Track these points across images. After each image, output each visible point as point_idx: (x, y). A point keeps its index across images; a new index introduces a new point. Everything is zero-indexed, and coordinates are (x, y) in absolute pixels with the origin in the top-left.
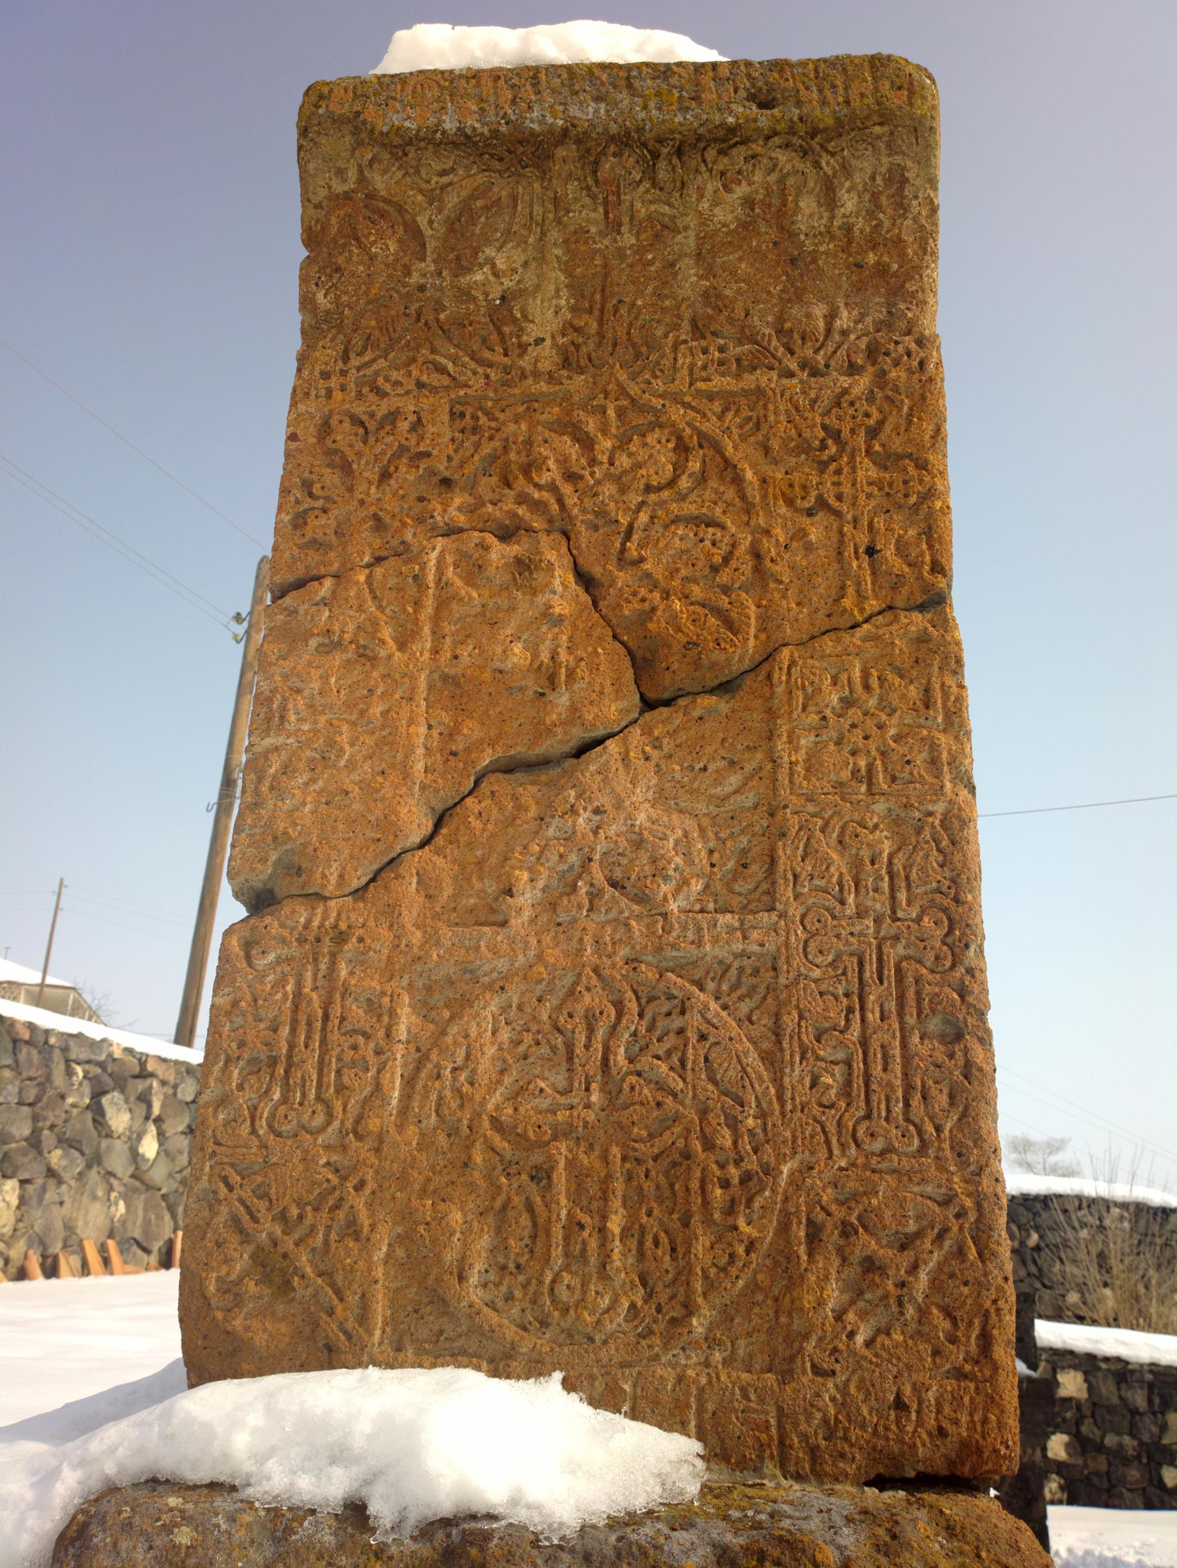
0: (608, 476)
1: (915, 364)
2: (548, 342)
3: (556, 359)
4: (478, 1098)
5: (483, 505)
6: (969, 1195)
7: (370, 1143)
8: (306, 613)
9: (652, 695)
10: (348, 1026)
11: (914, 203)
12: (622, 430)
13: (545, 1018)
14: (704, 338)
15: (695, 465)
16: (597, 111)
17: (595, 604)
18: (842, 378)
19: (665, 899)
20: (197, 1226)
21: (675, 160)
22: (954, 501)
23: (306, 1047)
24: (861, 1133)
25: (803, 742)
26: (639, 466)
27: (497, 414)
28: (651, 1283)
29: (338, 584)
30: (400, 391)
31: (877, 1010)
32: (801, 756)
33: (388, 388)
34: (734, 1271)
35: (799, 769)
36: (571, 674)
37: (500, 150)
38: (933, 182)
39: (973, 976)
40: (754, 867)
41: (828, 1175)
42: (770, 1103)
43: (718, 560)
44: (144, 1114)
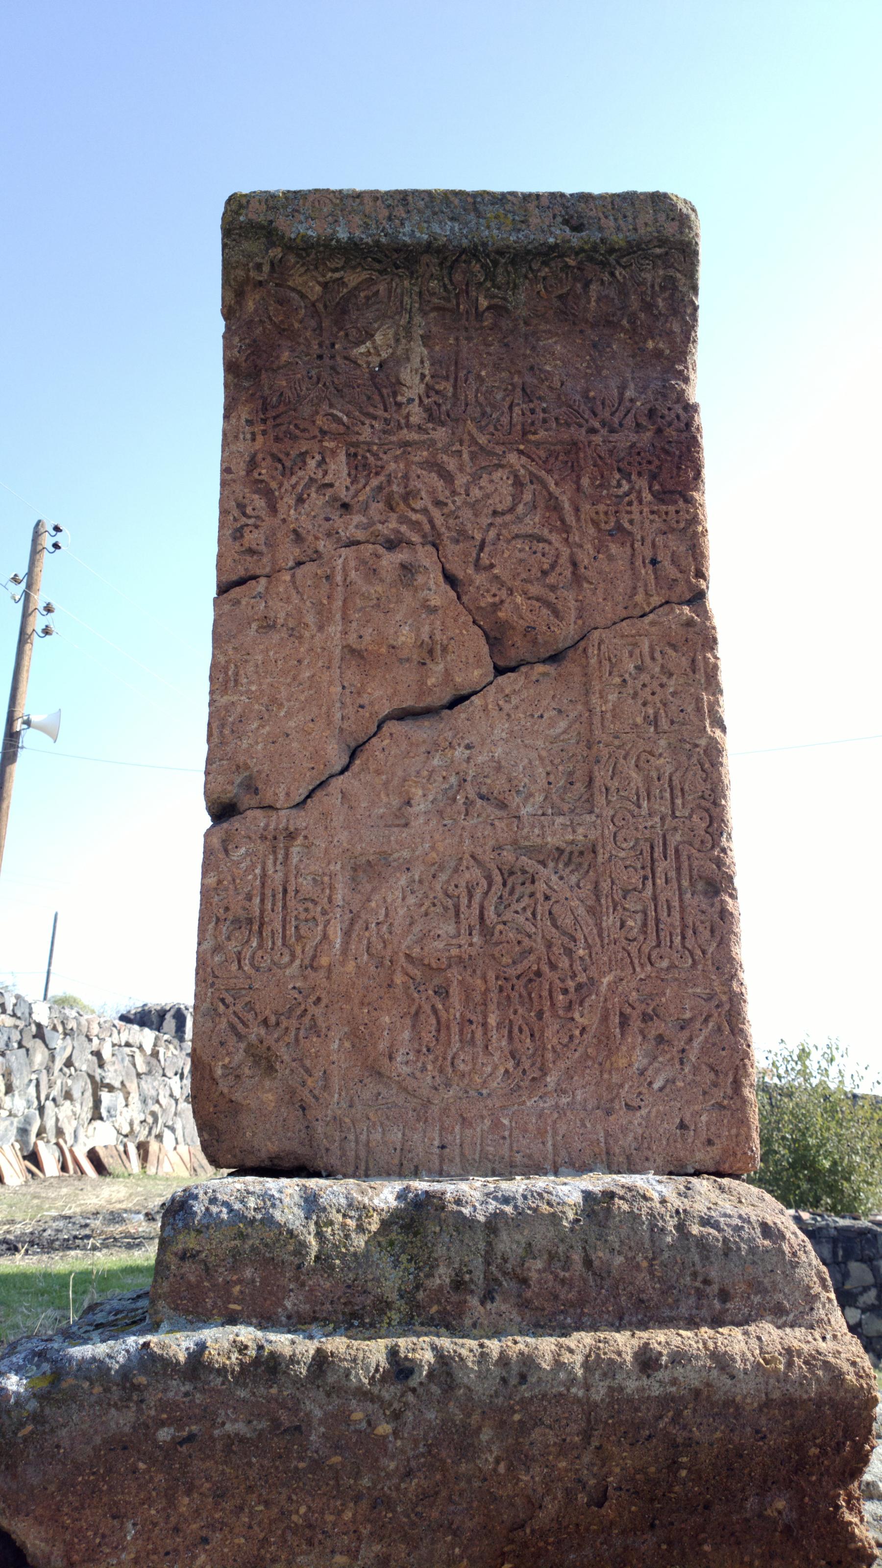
0: (465, 503)
2: (417, 401)
3: (425, 415)
4: (395, 941)
5: (374, 524)
6: (725, 993)
7: (322, 973)
8: (248, 603)
9: (501, 663)
10: (300, 896)
12: (474, 469)
13: (438, 887)
14: (531, 401)
15: (527, 497)
16: (452, 229)
17: (459, 598)
18: (631, 434)
19: (518, 806)
20: (204, 1033)
21: (510, 268)
22: (709, 525)
23: (273, 911)
24: (653, 957)
25: (610, 697)
26: (488, 496)
27: (381, 455)
28: (518, 1057)
29: (269, 583)
30: (307, 435)
34: (573, 1046)
35: (608, 715)
36: (444, 649)
37: (379, 256)
38: (695, 289)
39: (726, 853)
41: (633, 984)
42: (594, 939)
43: (546, 567)
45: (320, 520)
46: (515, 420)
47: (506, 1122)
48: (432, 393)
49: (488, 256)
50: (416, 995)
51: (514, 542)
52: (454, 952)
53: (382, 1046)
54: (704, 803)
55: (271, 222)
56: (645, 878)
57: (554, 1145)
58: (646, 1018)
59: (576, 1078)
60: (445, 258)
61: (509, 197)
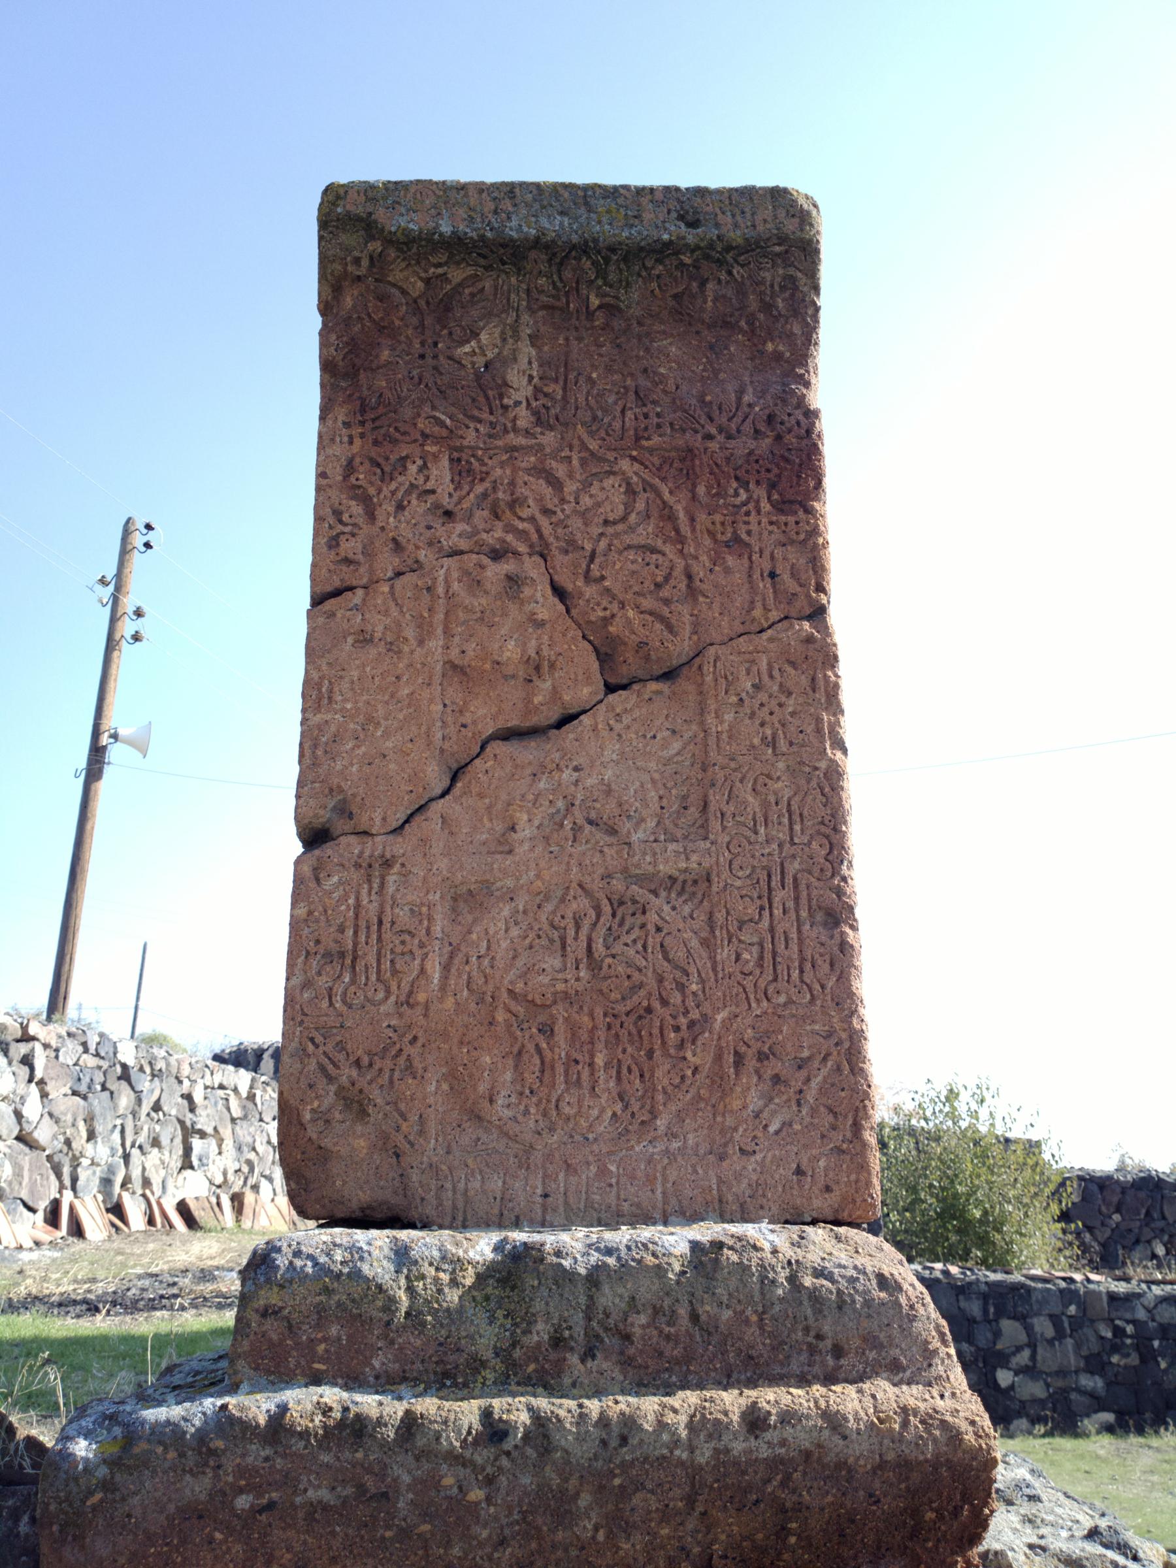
0: (575, 511)
2: (524, 404)
3: (533, 419)
4: (497, 976)
5: (478, 533)
6: (845, 1030)
7: (419, 1010)
8: (344, 616)
9: (612, 680)
10: (397, 928)
12: (584, 476)
13: (543, 918)
14: (645, 405)
15: (640, 505)
16: (561, 224)
17: (568, 611)
18: (749, 441)
19: (629, 832)
20: (292, 1074)
21: (622, 266)
22: (830, 537)
23: (367, 944)
25: (726, 717)
26: (598, 505)
27: (486, 460)
28: (626, 1099)
29: (367, 594)
30: (407, 438)
31: (781, 907)
32: (726, 726)
35: (724, 736)
36: (552, 666)
37: (484, 251)
38: (816, 289)
39: (846, 882)
40: (692, 809)
41: (749, 1021)
42: (707, 973)
43: (659, 579)
44: (27, 1077)
45: (421, 528)
46: (627, 424)
47: (613, 1168)
48: (540, 396)
49: (599, 252)
50: (519, 1033)
51: (626, 553)
52: (560, 987)
53: (482, 1088)
54: (823, 829)
55: (370, 214)
56: (762, 908)
57: (664, 1193)
58: (762, 1057)
59: (687, 1121)
60: (554, 254)
61: (622, 191)
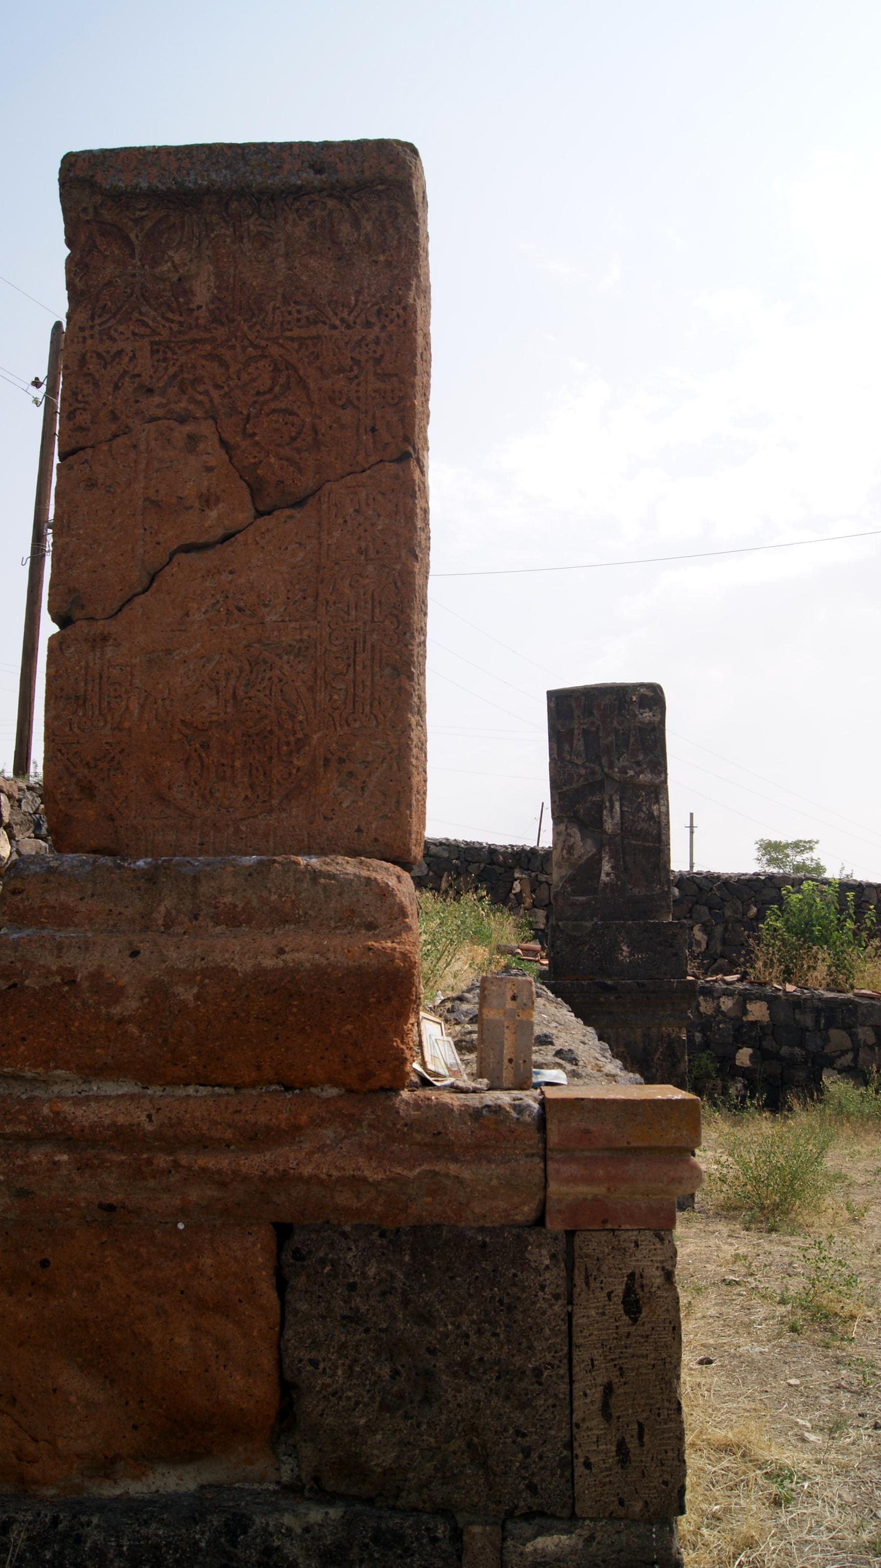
1: (401, 322)
2: (204, 308)
9: (261, 508)
11: (404, 226)
15: (282, 380)
21: (271, 204)
26: (254, 380)
33: (116, 335)
47: (243, 828)
50: (188, 747)
52: (214, 718)
55: (92, 176)
56: (349, 665)
58: (341, 761)
61: (269, 148)
